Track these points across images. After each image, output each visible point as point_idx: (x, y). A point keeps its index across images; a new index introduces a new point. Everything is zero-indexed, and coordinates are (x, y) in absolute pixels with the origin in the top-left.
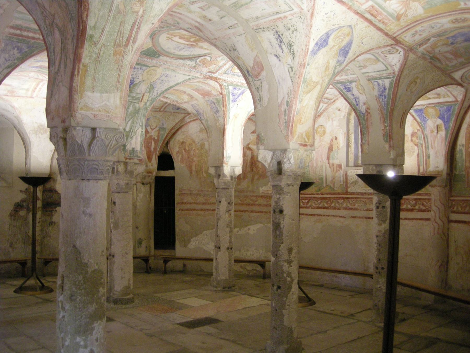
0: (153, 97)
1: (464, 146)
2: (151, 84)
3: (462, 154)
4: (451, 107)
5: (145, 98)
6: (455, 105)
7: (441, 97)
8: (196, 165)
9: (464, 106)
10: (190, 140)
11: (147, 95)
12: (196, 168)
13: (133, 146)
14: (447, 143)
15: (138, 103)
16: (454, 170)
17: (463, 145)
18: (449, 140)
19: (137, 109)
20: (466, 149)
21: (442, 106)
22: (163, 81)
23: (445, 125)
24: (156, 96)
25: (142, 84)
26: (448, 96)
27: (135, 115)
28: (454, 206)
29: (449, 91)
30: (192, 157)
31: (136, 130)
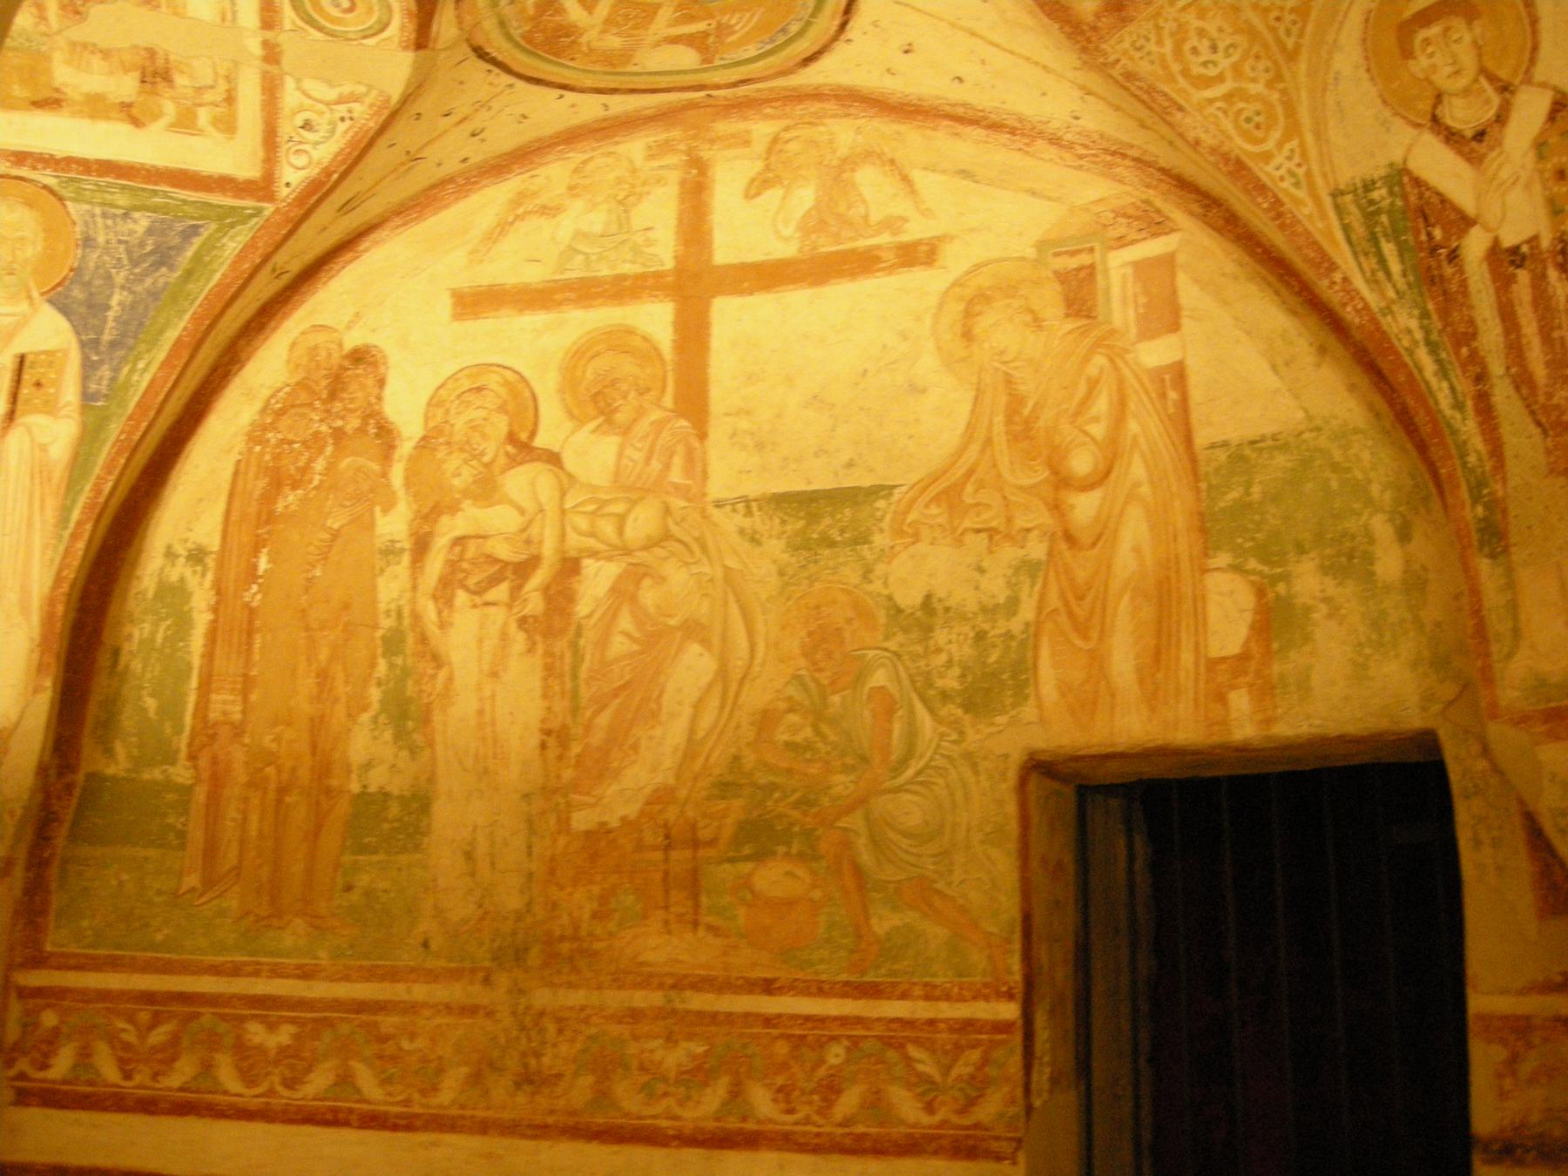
1: (211, 562)
3: (183, 623)
4: (194, 231)
6: (228, 219)
7: (156, 116)
9: (280, 259)
14: (76, 515)
16: (88, 745)
17: (197, 556)
18: (97, 490)
20: (218, 588)
21: (123, 200)
23: (88, 368)
26: (216, 122)
28: (53, 1040)
29: (272, 54)
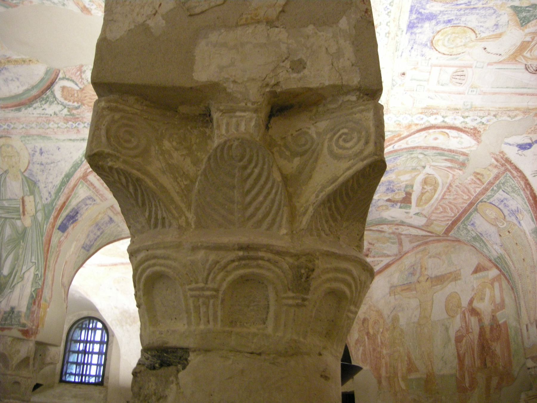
0: (45, 202)
2: (26, 177)
5: (30, 206)
8: (386, 364)
10: (375, 312)
11: (29, 200)
12: (387, 373)
13: (14, 302)
15: (20, 219)
19: (20, 230)
22: (42, 164)
24: (49, 199)
25: (7, 179)
27: (20, 242)
30: (379, 349)
31: (23, 272)
